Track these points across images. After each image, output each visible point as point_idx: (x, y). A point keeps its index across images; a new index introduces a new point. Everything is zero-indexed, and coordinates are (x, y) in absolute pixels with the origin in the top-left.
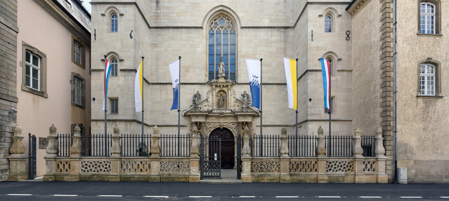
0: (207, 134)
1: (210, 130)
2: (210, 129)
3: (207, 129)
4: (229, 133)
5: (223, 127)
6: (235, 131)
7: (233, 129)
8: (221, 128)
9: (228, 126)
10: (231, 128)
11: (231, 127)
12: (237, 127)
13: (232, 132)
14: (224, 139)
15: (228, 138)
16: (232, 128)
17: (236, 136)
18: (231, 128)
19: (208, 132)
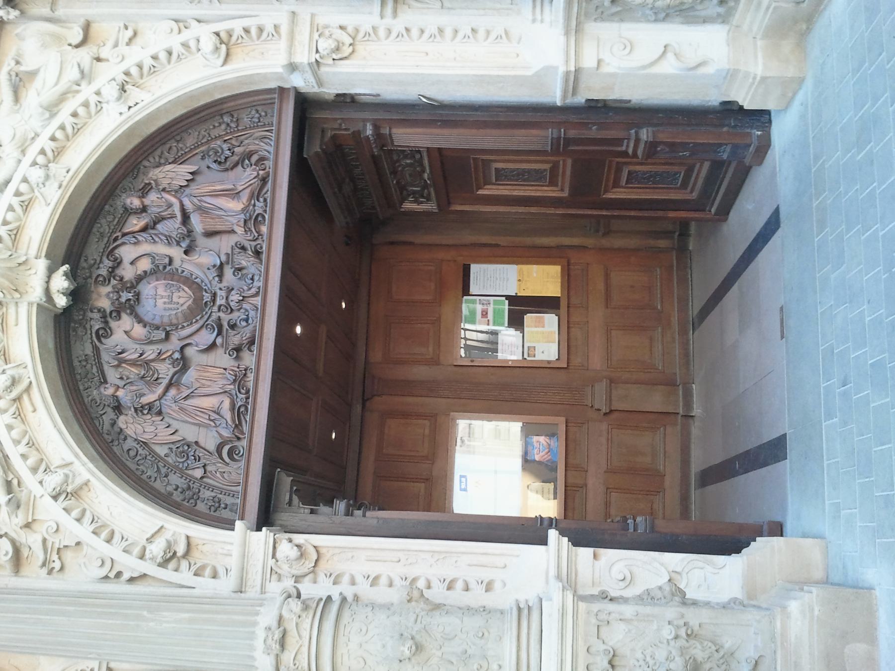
0: (114, 551)
1: (54, 481)
2: (30, 481)
3: (32, 540)
4: (178, 173)
5: (33, 252)
6: (138, 54)
7: (87, 92)
8: (60, 282)
9: (36, 174)
10: (64, 116)
11: (52, 109)
12: (76, 35)
13: (138, 115)
14: (257, 253)
15: (257, 195)
16: (72, 104)
17: (208, 43)
18: (64, 116)
19: (83, 532)
